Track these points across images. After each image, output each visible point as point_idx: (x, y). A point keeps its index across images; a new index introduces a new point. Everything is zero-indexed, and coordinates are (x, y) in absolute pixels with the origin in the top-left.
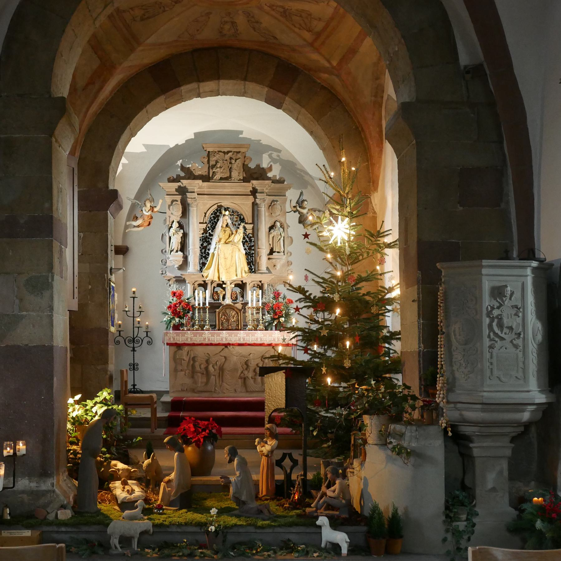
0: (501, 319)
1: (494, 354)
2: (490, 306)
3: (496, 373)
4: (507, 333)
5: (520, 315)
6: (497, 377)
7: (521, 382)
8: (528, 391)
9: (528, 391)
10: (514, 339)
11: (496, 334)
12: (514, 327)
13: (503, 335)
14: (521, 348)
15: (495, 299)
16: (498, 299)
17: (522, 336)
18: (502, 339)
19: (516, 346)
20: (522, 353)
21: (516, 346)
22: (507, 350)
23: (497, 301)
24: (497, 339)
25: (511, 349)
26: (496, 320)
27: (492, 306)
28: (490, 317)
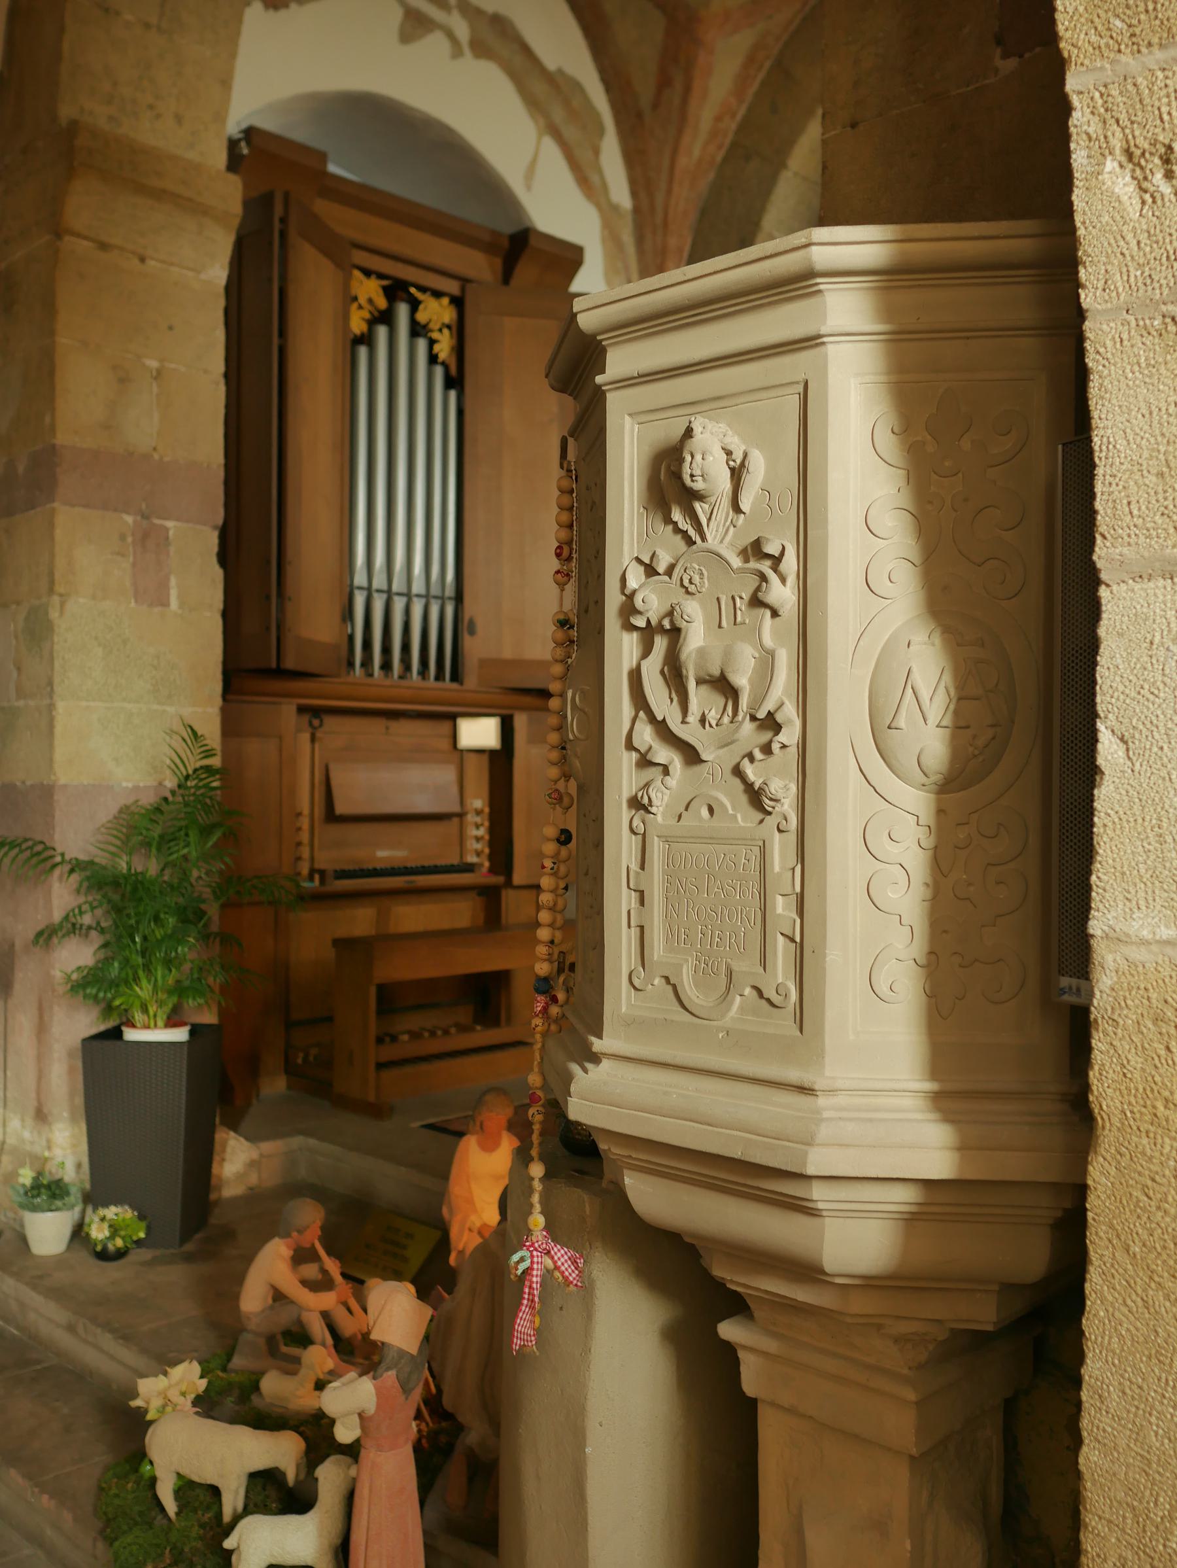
0: (675, 633)
1: (657, 848)
2: (639, 560)
3: (658, 949)
4: (712, 716)
5: (782, 594)
6: (667, 979)
7: (785, 1024)
8: (804, 1090)
9: (804, 1090)
10: (751, 757)
11: (662, 729)
12: (742, 680)
13: (688, 732)
14: (787, 806)
15: (668, 520)
16: (677, 515)
17: (790, 735)
18: (691, 755)
19: (756, 797)
20: (792, 838)
21: (756, 797)
22: (716, 823)
23: (677, 530)
24: (663, 754)
25: (744, 817)
26: (660, 644)
27: (647, 561)
28: (636, 628)
